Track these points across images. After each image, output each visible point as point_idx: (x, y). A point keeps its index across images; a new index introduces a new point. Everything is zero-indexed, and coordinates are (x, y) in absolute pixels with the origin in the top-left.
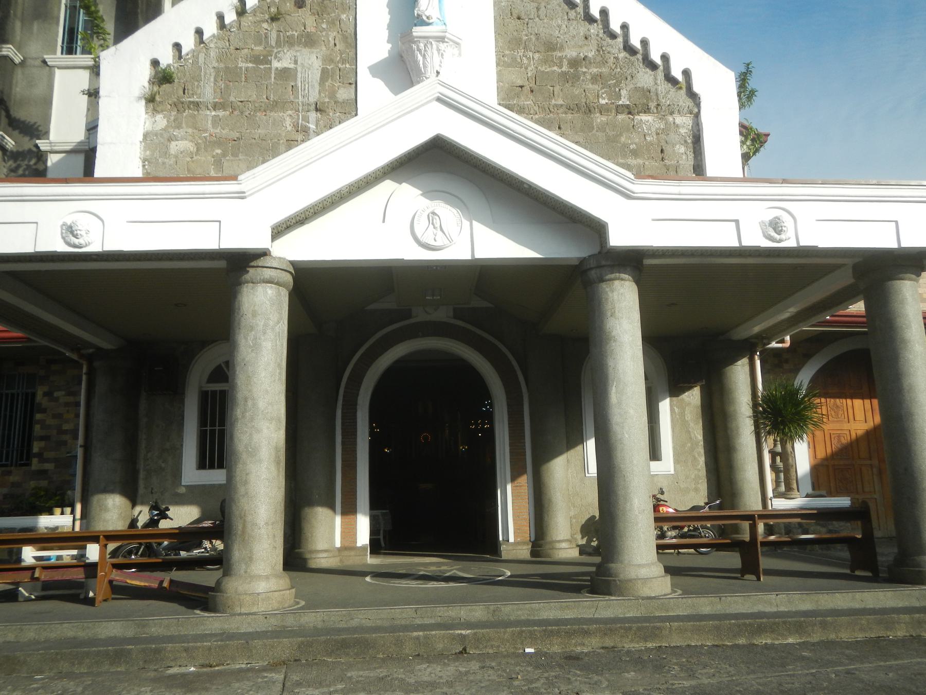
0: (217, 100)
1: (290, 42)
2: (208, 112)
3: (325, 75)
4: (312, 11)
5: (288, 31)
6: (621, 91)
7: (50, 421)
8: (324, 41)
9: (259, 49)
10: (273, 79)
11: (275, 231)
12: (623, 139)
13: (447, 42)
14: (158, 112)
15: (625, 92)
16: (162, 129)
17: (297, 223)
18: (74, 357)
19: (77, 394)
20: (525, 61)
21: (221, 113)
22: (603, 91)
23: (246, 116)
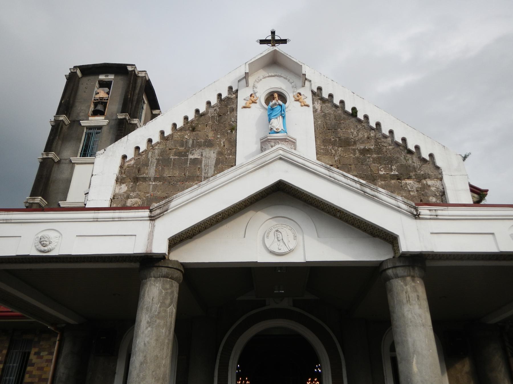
0: (156, 176)
2: (151, 183)
4: (212, 129)
5: (199, 140)
6: (392, 166)
7: (35, 372)
8: (218, 144)
10: (188, 165)
11: (173, 242)
13: (287, 142)
14: (124, 183)
15: (395, 167)
16: (124, 192)
17: (187, 237)
18: (52, 329)
19: (51, 354)
20: (333, 152)
21: (158, 183)
22: (381, 167)
23: (172, 185)
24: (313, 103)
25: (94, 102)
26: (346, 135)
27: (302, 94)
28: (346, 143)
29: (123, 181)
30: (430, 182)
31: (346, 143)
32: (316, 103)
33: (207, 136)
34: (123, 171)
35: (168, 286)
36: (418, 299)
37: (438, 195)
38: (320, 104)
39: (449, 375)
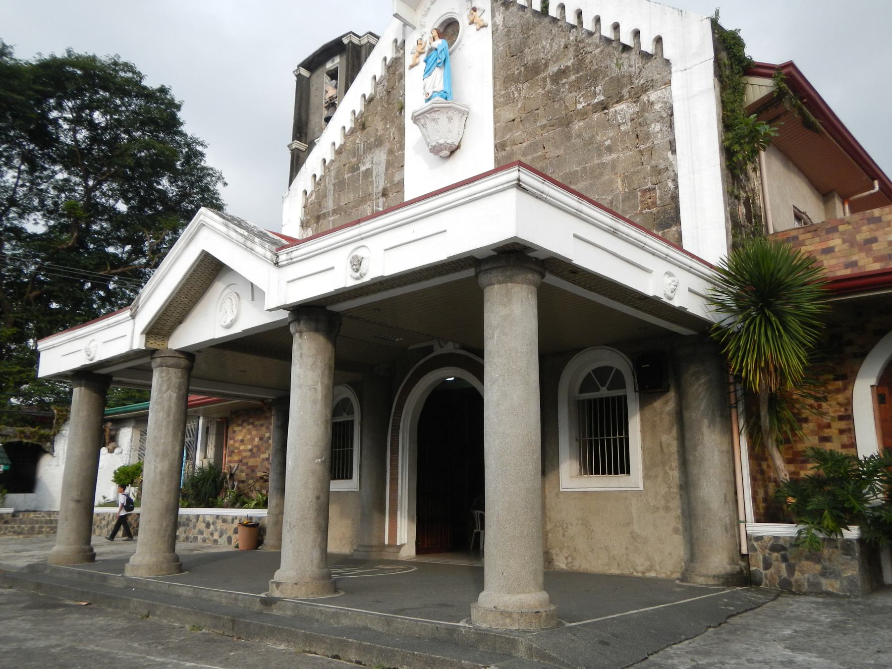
1: (369, 148)
3: (389, 165)
9: (354, 160)
10: (361, 181)
12: (599, 138)
13: (438, 111)
14: (309, 227)
22: (580, 95)
24: (493, 16)
25: (326, 107)
26: (535, 57)
27: (477, 7)
28: (533, 71)
29: (308, 225)
30: (653, 96)
31: (533, 71)
32: (497, 13)
33: (377, 130)
34: (307, 211)
35: (164, 374)
36: (301, 357)
37: (664, 116)
38: (502, 13)
39: (642, 420)
